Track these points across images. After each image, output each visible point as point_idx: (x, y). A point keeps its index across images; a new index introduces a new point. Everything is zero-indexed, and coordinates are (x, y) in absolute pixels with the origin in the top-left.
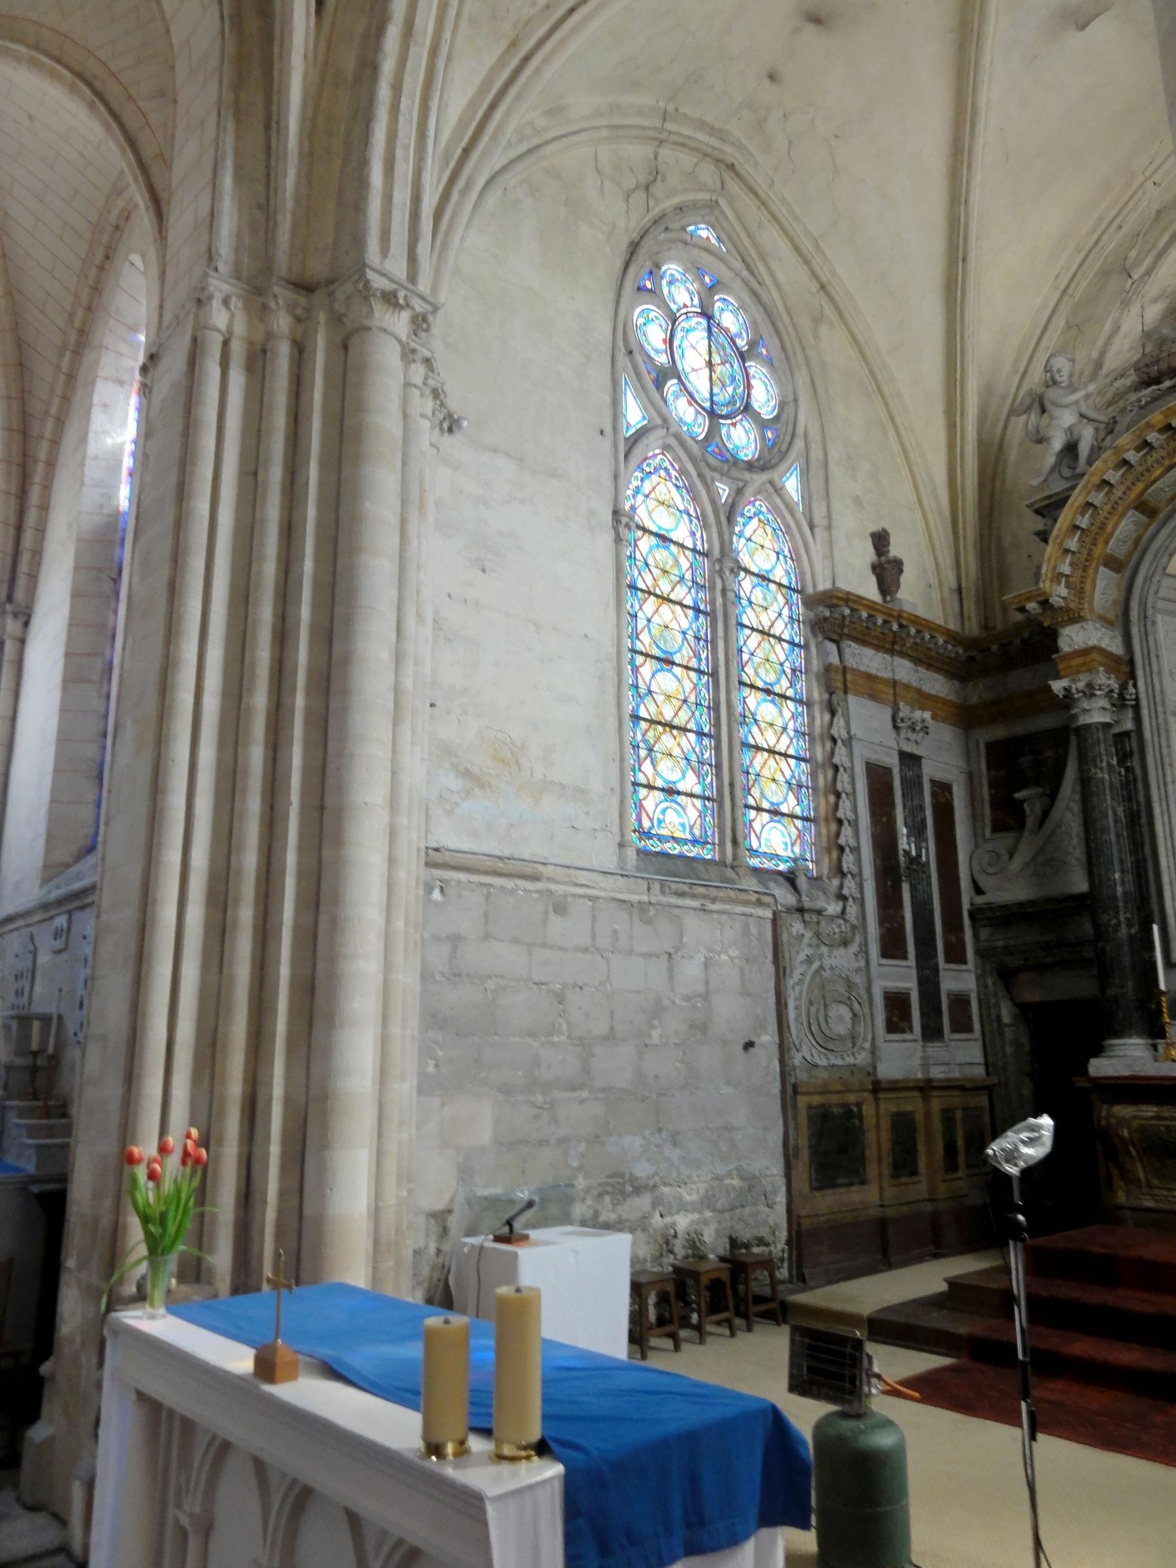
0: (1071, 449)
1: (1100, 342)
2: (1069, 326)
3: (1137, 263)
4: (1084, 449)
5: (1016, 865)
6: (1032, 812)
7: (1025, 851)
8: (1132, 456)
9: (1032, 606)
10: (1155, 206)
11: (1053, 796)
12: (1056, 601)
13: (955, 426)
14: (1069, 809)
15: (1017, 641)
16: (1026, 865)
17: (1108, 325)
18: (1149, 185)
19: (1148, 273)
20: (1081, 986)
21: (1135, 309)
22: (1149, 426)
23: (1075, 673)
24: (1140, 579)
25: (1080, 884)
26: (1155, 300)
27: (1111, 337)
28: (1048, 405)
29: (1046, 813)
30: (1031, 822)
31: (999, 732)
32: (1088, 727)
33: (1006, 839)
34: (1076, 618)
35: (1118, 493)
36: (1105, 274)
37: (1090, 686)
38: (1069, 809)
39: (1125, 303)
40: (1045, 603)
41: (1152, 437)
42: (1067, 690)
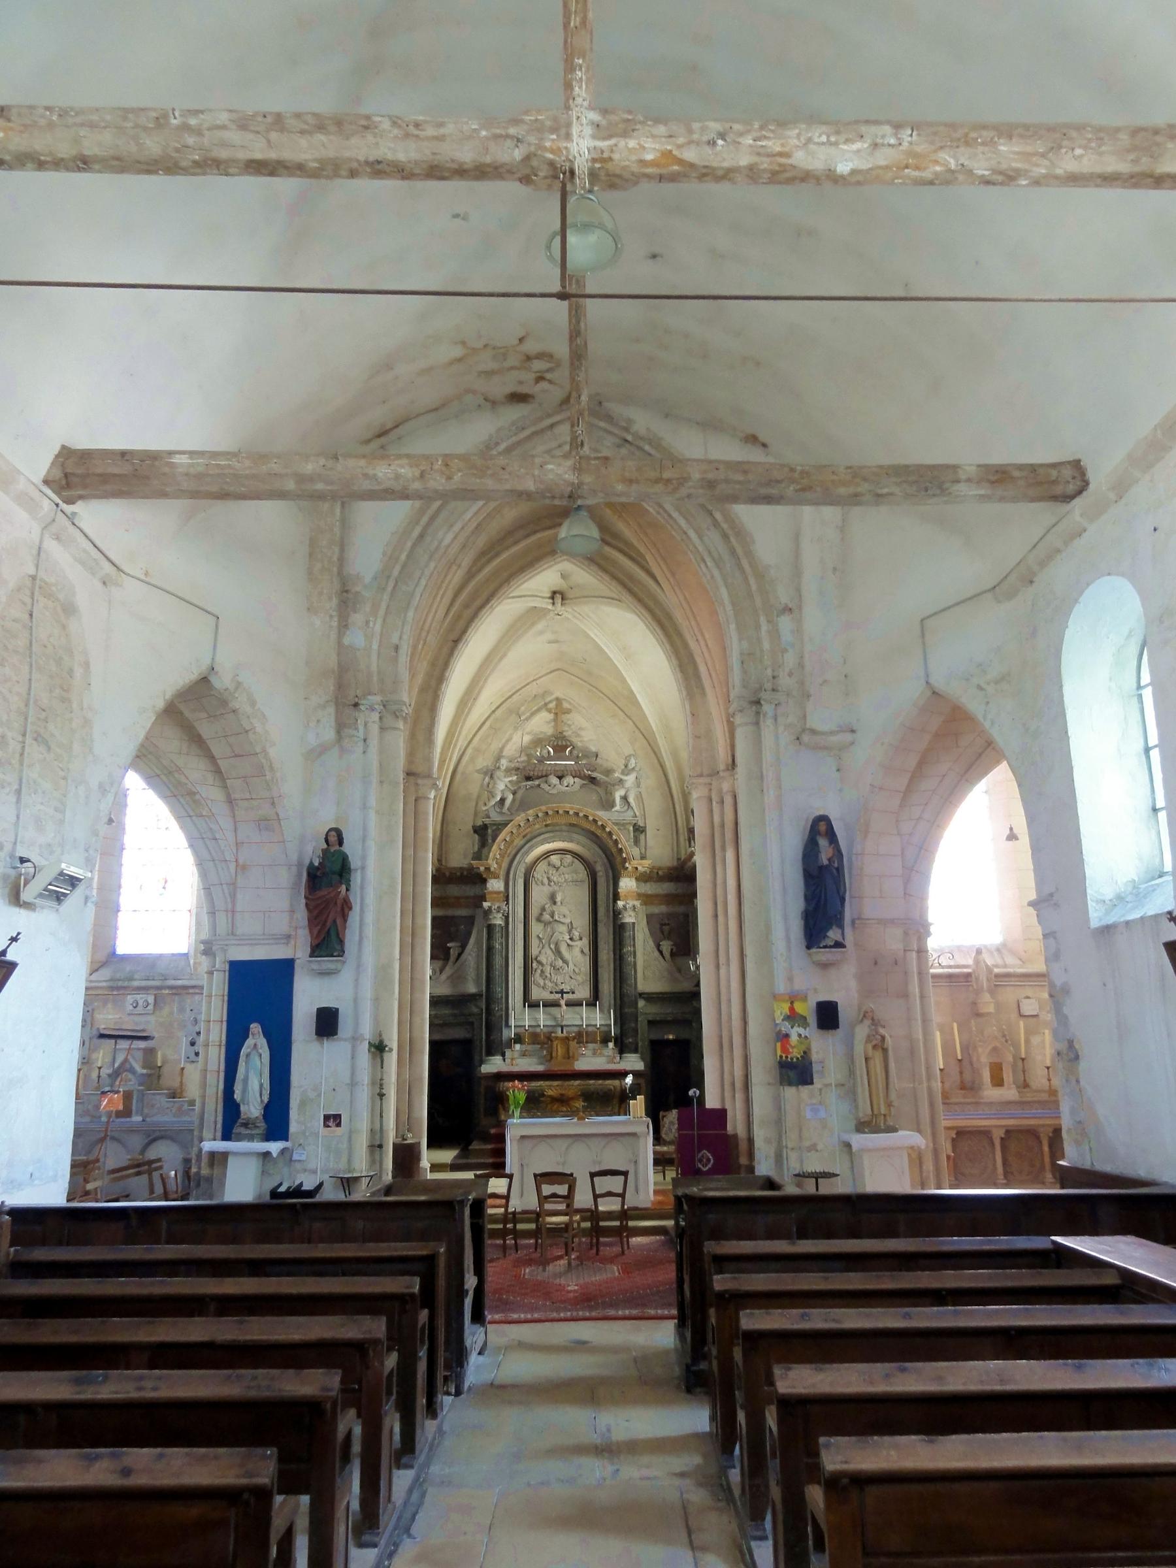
0: (502, 800)
1: (504, 741)
2: (491, 727)
3: (524, 713)
4: (508, 802)
5: (444, 976)
6: (453, 953)
7: (448, 971)
8: (531, 819)
9: (482, 869)
10: (534, 693)
11: (463, 947)
12: (492, 869)
13: (445, 761)
14: (470, 954)
15: (458, 874)
16: (448, 978)
17: (507, 736)
18: (535, 683)
19: (527, 719)
20: (459, 1033)
21: (519, 733)
22: (540, 810)
23: (493, 900)
24: (515, 862)
25: (472, 989)
26: (528, 733)
27: (508, 741)
28: (495, 777)
29: (460, 955)
30: (452, 959)
31: (440, 913)
32: (495, 925)
33: (439, 963)
34: (496, 877)
35: (521, 830)
36: (510, 711)
37: (499, 907)
38: (470, 954)
39: (516, 729)
40: (488, 869)
41: (540, 815)
42: (490, 908)
